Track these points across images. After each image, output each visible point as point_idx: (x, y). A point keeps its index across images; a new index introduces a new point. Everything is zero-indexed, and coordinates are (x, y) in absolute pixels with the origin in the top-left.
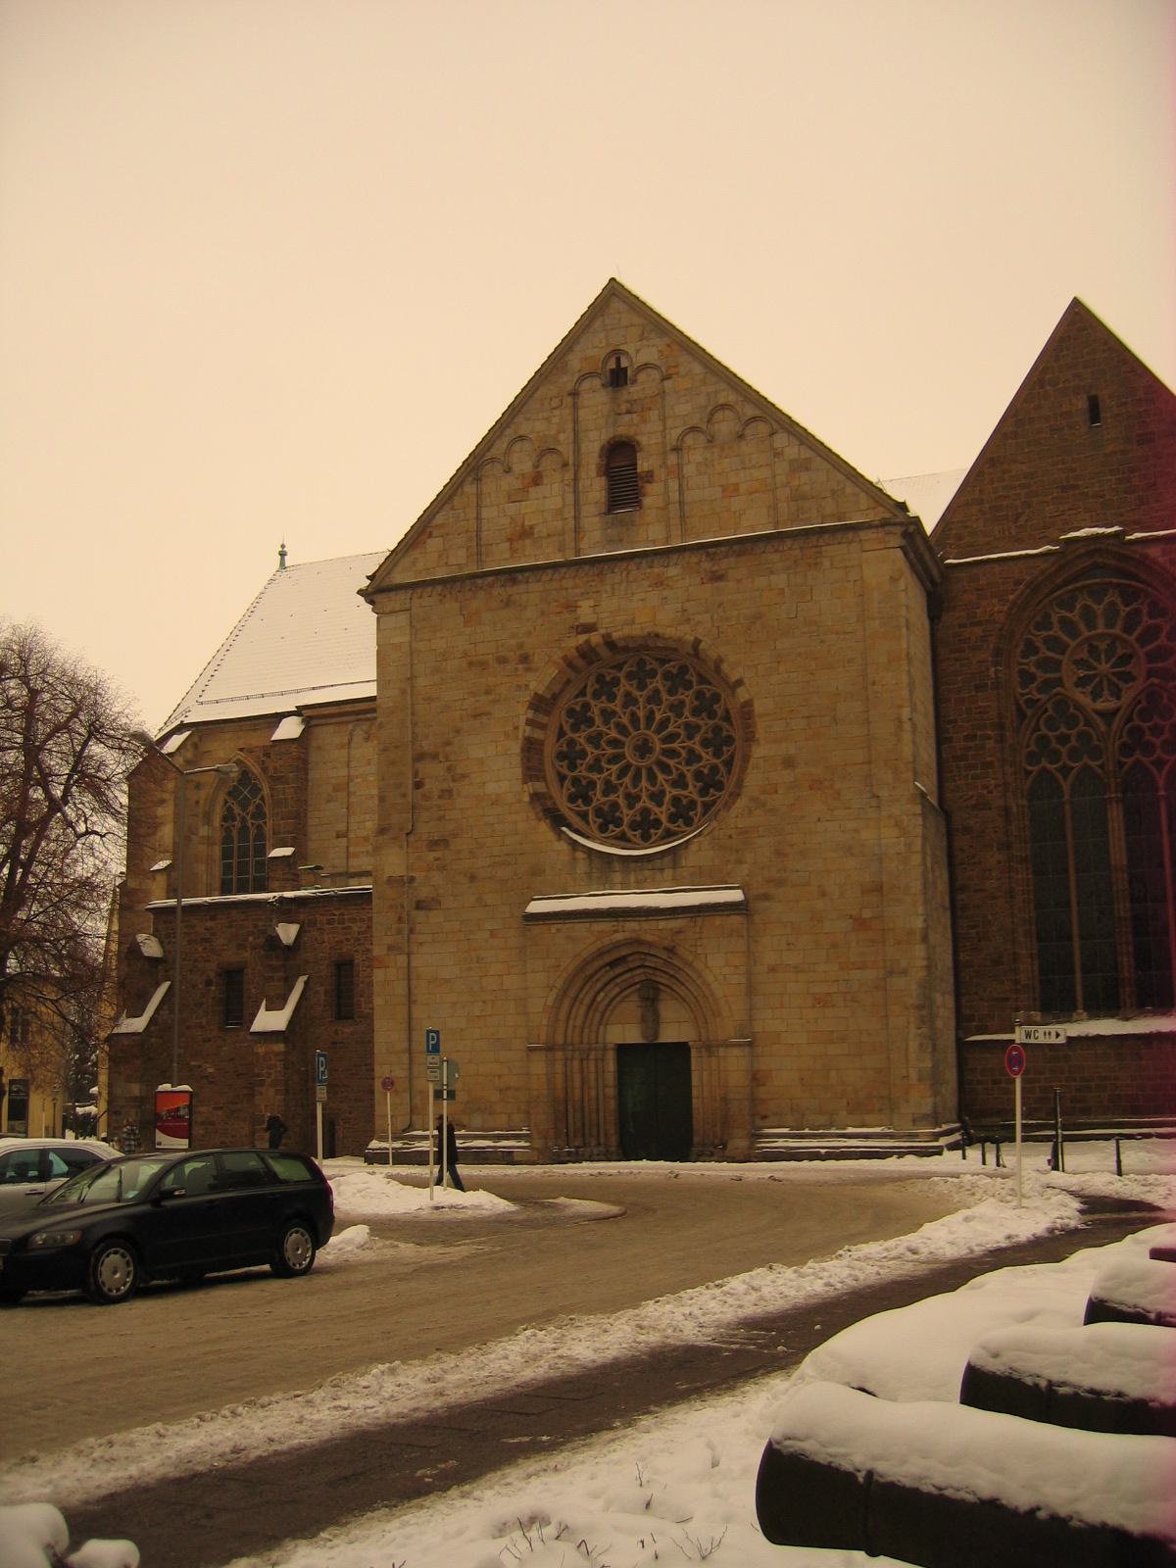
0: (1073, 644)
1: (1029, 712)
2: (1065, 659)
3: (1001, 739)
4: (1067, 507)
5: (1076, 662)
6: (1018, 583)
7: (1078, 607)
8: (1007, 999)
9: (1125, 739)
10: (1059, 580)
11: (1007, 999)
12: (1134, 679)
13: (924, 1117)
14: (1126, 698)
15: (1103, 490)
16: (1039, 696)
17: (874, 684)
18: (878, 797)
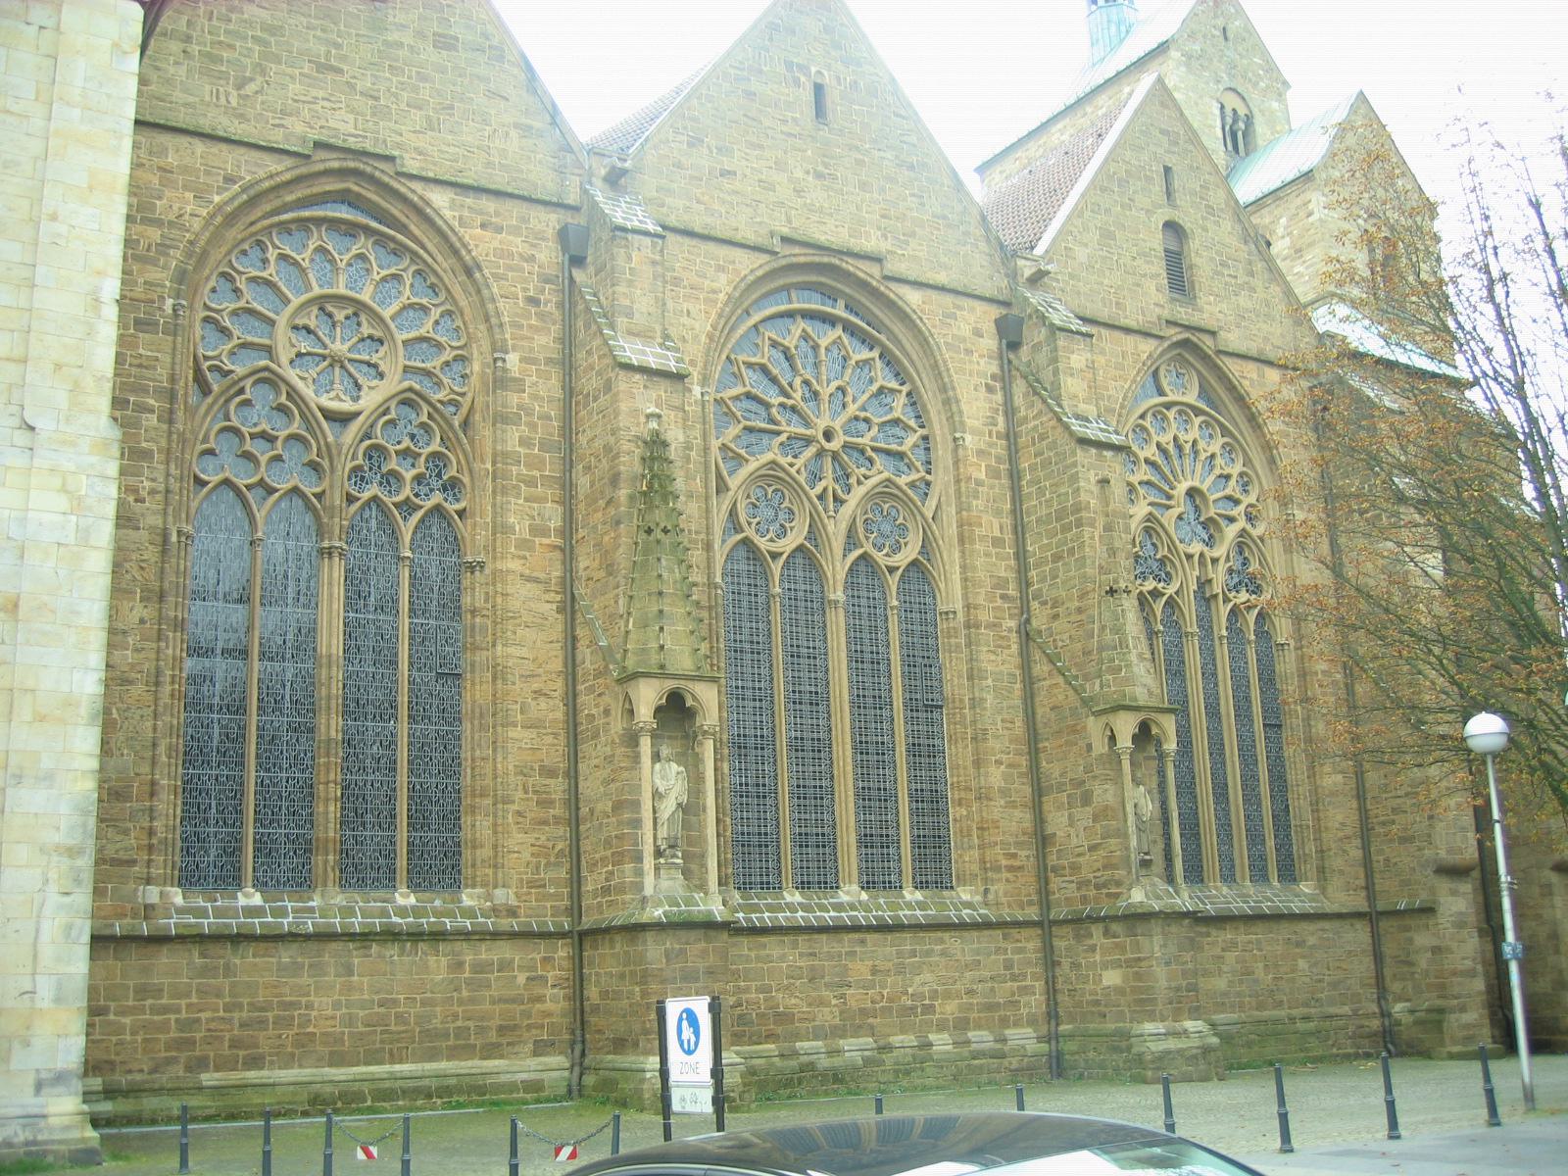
0: (296, 301)
1: (215, 388)
2: (282, 321)
3: (169, 418)
4: (321, 94)
5: (295, 328)
6: (230, 180)
7: (312, 247)
8: (132, 862)
9: (360, 461)
10: (289, 198)
11: (132, 862)
12: (381, 376)
13: (60, 1078)
14: (369, 400)
15: (379, 91)
16: (233, 368)
17: (54, 218)
18: (32, 429)
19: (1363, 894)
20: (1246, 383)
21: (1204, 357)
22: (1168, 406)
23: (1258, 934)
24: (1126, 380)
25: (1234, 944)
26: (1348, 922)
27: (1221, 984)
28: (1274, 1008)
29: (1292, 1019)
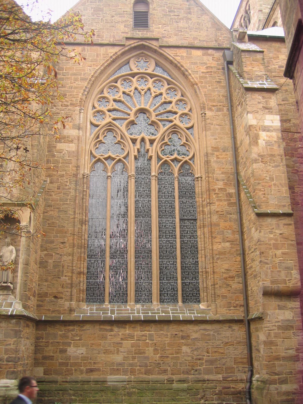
19: (242, 309)
20: (178, 58)
21: (155, 51)
22: (133, 75)
23: (152, 331)
24: (97, 66)
25: (132, 337)
26: (227, 325)
27: (119, 358)
28: (159, 374)
29: (171, 381)
